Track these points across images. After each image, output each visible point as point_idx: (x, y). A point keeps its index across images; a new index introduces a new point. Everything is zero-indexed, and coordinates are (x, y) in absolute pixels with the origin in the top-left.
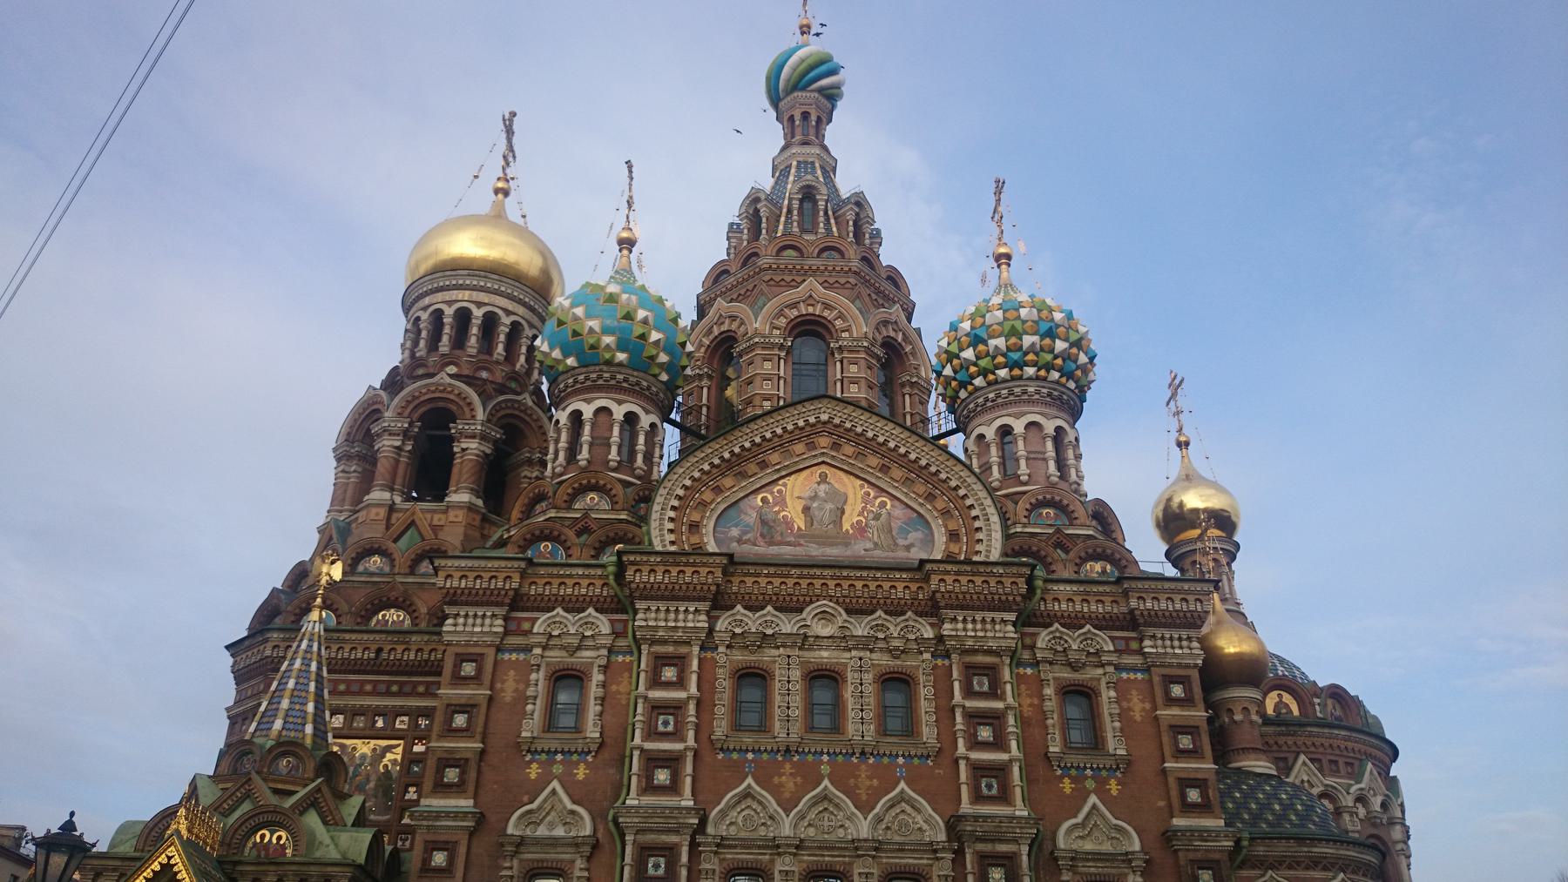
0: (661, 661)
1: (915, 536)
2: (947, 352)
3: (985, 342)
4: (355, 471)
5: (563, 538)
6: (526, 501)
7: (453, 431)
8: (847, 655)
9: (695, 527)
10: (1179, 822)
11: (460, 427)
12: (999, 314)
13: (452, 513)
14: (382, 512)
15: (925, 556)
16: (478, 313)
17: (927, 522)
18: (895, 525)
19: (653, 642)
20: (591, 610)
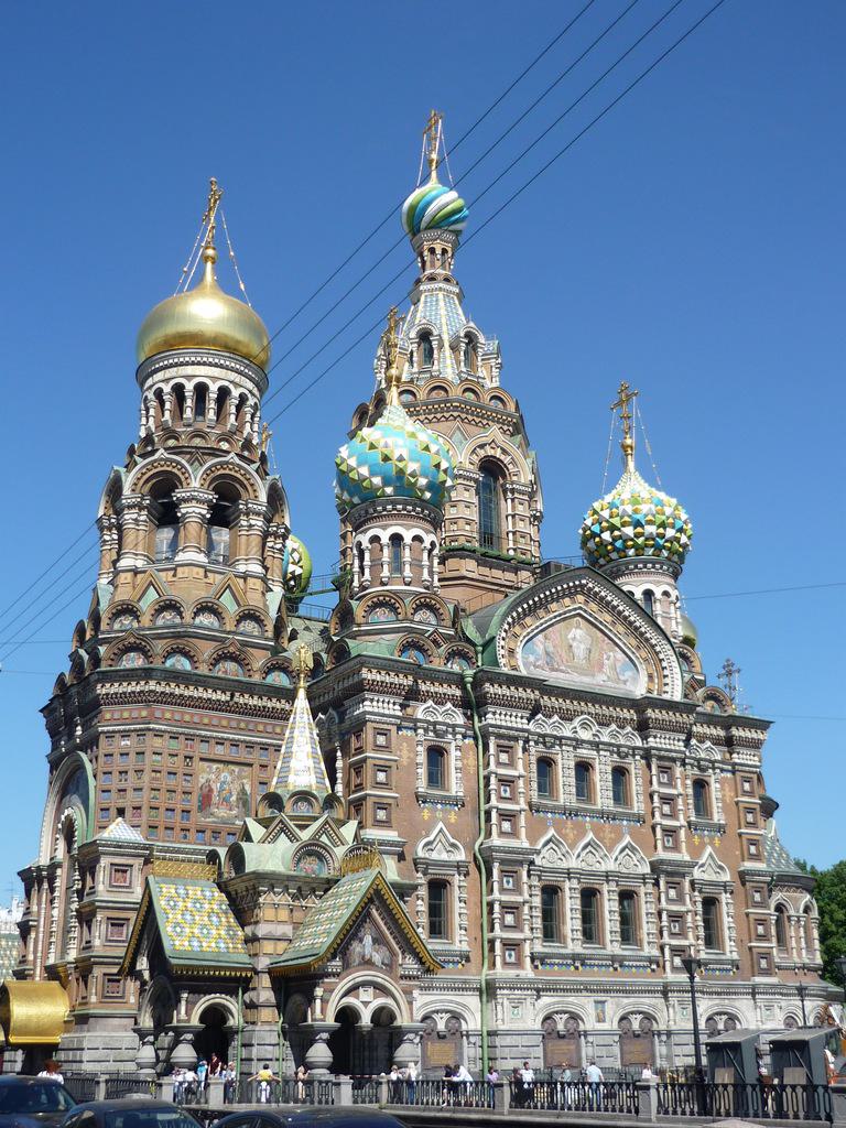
0: (501, 749)
1: (629, 674)
2: (607, 521)
3: (642, 526)
4: (145, 521)
5: (426, 647)
6: (370, 603)
7: (241, 507)
8: (595, 752)
9: (512, 652)
10: (749, 865)
11: (250, 505)
12: (653, 507)
13: (250, 580)
14: (201, 571)
15: (632, 688)
16: (235, 393)
17: (635, 666)
18: (618, 665)
19: (499, 736)
20: (449, 705)
